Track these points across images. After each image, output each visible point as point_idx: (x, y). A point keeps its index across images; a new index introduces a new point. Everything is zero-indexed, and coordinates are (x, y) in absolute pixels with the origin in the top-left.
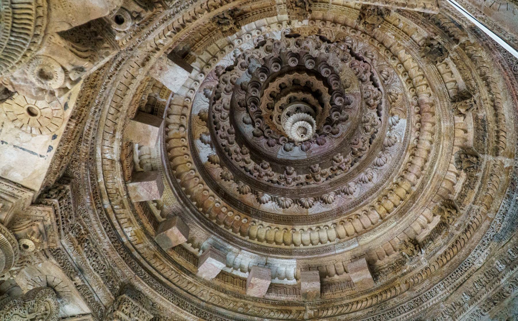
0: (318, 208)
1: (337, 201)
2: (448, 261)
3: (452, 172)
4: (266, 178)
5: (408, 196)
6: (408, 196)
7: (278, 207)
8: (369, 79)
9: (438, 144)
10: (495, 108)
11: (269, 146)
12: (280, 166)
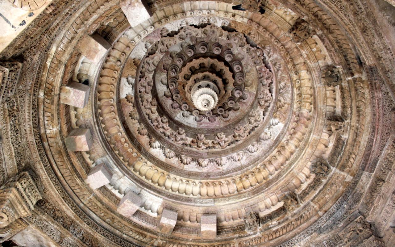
0: (192, 167)
1: (208, 167)
3: (304, 173)
4: (162, 130)
5: (264, 181)
6: (264, 181)
7: (163, 155)
8: (268, 85)
9: (302, 150)
10: (357, 135)
11: (172, 107)
12: (175, 125)
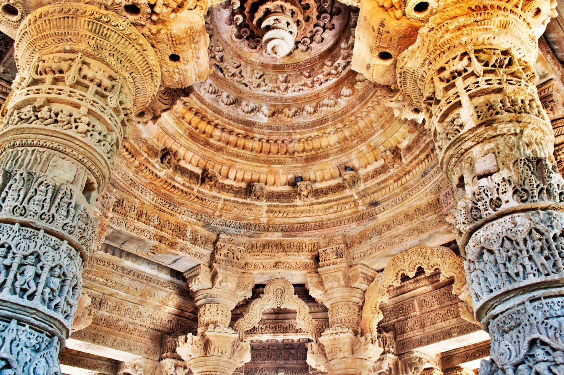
2: (168, 190)
